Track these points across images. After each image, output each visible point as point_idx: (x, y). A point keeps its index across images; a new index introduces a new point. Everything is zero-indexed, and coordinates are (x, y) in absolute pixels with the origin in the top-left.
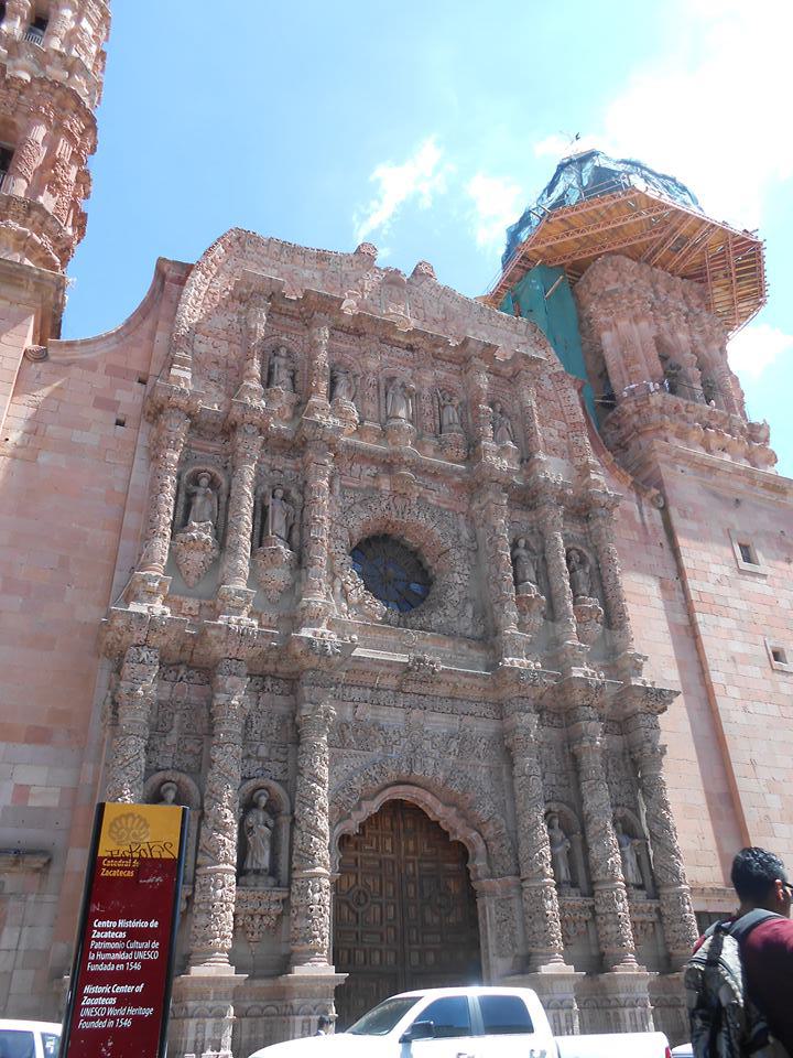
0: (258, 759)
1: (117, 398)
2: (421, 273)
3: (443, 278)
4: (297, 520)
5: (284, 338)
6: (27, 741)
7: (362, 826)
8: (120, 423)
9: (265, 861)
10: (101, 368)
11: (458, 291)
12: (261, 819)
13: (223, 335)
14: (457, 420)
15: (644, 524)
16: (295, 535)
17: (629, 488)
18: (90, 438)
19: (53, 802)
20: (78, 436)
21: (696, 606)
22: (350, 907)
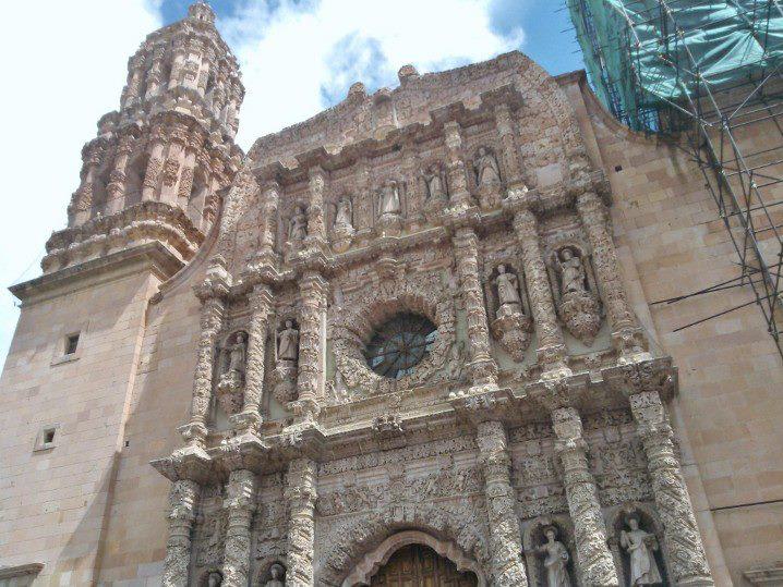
2: (407, 74)
5: (300, 199)
6: (154, 561)
15: (681, 175)
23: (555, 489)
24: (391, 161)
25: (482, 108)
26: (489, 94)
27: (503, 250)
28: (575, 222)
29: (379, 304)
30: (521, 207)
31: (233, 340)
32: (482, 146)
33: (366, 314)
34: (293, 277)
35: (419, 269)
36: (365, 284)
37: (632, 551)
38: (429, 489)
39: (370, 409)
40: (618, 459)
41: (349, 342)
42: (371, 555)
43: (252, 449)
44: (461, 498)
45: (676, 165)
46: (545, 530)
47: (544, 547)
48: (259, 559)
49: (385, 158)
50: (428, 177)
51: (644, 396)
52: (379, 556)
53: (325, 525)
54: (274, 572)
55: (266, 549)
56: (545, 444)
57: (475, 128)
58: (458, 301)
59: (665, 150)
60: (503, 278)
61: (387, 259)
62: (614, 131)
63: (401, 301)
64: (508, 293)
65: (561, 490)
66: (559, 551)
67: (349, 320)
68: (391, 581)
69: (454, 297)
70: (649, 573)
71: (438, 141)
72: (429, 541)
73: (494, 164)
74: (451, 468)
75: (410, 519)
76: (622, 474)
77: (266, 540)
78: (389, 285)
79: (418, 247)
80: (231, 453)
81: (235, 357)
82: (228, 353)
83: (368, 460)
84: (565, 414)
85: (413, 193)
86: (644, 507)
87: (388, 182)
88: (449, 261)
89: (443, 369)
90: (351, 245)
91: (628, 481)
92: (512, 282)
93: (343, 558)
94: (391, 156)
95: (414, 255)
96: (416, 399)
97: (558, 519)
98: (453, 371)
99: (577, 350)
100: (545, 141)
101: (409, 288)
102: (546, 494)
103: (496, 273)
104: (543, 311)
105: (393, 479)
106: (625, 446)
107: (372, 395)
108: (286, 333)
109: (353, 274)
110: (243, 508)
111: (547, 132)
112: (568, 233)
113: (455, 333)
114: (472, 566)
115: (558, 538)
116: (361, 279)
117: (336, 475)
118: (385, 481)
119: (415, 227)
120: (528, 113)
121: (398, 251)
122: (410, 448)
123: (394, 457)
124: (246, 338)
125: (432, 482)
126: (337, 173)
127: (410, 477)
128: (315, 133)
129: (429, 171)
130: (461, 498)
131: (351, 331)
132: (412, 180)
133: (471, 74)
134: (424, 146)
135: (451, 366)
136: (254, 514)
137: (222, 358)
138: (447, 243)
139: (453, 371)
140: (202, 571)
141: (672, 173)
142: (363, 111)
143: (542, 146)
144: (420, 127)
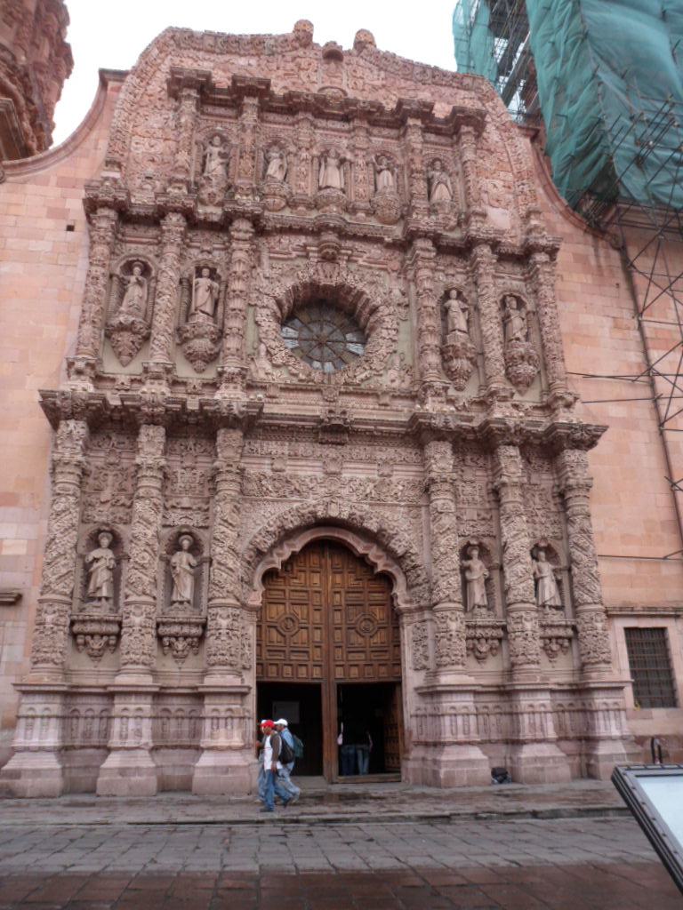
0: (183, 508)
1: (67, 206)
2: (364, 42)
3: (383, 45)
4: (222, 295)
5: (219, 128)
7: (284, 564)
8: (70, 228)
9: (187, 594)
10: (53, 180)
11: (398, 54)
12: (184, 560)
13: (159, 134)
14: (391, 183)
15: (599, 266)
16: (220, 309)
17: (585, 231)
18: (43, 246)
19: (22, 551)
20: (35, 246)
21: (650, 343)
22: (278, 631)
23: (483, 515)
24: (337, 130)
25: (447, 121)
26: (462, 110)
27: (453, 275)
28: (523, 274)
29: (313, 286)
30: (486, 242)
31: (128, 268)
32: (439, 160)
33: (295, 288)
34: (215, 219)
35: (361, 261)
36: (298, 256)
37: (542, 578)
38: (368, 491)
39: (301, 395)
40: (537, 499)
41: (274, 315)
42: (291, 542)
43: (179, 406)
44: (397, 505)
45: (597, 256)
46: (469, 549)
47: (470, 562)
48: (165, 526)
49: (330, 124)
50: (379, 168)
51: (577, 452)
52: (298, 544)
53: (248, 505)
54: (186, 543)
55: (177, 518)
56: (479, 473)
57: (432, 137)
58: (401, 310)
59: (590, 238)
60: (454, 304)
61: (331, 237)
62: (553, 202)
63: (341, 287)
64: (461, 322)
65: (488, 517)
66: (481, 568)
67: (280, 292)
68: (300, 571)
69: (399, 305)
70: (554, 598)
71: (394, 132)
72: (350, 539)
73: (449, 183)
74: (389, 476)
75: (345, 516)
76: (539, 513)
77: (173, 507)
78: (328, 267)
79: (365, 239)
80: (154, 405)
81: (135, 293)
82: (123, 285)
83: (302, 448)
84: (513, 451)
85: (361, 177)
86: (554, 544)
87: (332, 153)
88: (396, 265)
89: (381, 375)
90: (284, 207)
91: (543, 520)
92: (464, 310)
93: (270, 541)
94: (338, 125)
95: (358, 245)
96: (353, 398)
97: (486, 541)
98: (393, 381)
99: (517, 397)
100: (499, 183)
102: (475, 518)
103: (447, 296)
104: (495, 351)
105: (329, 474)
106: (543, 489)
107: (301, 380)
108: (204, 282)
109: (285, 240)
110: (161, 468)
111: (502, 173)
112: (515, 283)
113: (394, 341)
114: (393, 570)
115: (480, 557)
116: (294, 250)
117: (262, 457)
118: (320, 475)
119: (361, 215)
120: (485, 147)
121: (342, 234)
122: (349, 447)
123: (332, 452)
124: (146, 270)
125: (372, 485)
126: (272, 117)
127: (346, 475)
128: (245, 55)
129: (377, 158)
130: (397, 505)
131: (279, 303)
132: (361, 162)
133: (434, 77)
134: (375, 131)
135: (393, 374)
136: (166, 477)
137: (115, 287)
138: (404, 245)
139: (393, 381)
140: (91, 528)
141: (593, 262)
142: (308, 58)
143: (495, 186)
144: (380, 108)
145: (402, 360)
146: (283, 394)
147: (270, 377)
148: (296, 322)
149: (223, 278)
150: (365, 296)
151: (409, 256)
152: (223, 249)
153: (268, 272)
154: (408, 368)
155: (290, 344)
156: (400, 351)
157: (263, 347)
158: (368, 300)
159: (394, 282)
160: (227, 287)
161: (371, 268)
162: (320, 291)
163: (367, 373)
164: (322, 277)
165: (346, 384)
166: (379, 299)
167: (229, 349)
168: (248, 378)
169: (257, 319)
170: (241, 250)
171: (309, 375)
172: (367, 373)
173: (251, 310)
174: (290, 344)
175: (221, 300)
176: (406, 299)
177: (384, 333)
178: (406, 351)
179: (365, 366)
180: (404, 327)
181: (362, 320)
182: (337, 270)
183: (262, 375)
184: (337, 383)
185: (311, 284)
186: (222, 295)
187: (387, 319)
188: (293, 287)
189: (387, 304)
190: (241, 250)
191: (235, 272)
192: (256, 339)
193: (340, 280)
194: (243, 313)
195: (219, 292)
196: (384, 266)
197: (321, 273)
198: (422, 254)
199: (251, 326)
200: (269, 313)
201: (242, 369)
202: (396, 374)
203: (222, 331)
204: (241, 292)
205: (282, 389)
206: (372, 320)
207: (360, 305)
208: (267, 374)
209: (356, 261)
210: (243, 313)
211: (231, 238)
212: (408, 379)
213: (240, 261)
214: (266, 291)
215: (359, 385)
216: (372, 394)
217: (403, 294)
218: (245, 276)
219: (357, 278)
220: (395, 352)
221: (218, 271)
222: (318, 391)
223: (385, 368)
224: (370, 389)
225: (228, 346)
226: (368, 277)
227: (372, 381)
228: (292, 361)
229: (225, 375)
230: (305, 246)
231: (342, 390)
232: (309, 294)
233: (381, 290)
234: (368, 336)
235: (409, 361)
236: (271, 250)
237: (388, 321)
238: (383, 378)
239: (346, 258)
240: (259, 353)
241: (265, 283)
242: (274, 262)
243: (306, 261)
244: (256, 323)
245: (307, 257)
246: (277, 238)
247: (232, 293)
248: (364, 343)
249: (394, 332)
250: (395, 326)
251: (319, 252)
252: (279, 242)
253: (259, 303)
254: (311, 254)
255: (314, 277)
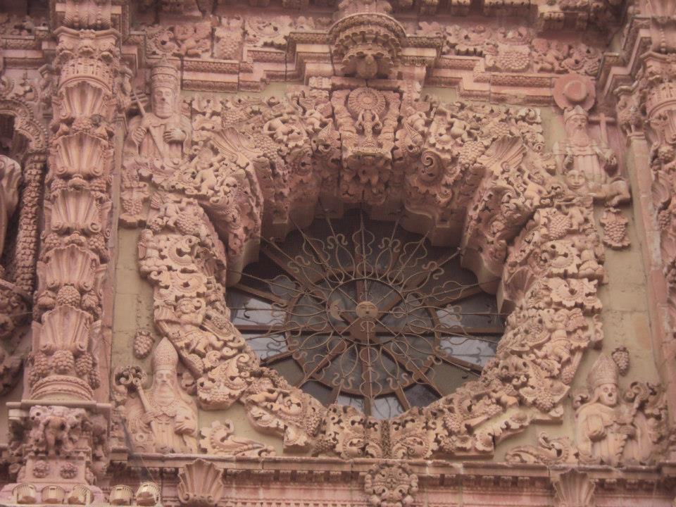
33: (267, 171)
35: (468, 81)
36: (272, 76)
41: (201, 251)
58: (608, 217)
69: (599, 203)
78: (365, 101)
88: (581, 85)
89: (557, 422)
98: (597, 439)
101: (437, 127)
107: (294, 449)
113: (591, 313)
116: (259, 59)
131: (215, 216)
135: (593, 416)
139: (597, 439)
145: (622, 372)
146: (233, 493)
147: (191, 442)
148: (281, 286)
149: (33, 145)
150: (487, 183)
151: (618, 52)
152: (34, 64)
153: (178, 125)
154: (643, 394)
155: (261, 348)
156: (611, 345)
157: (165, 353)
158: (499, 192)
159: (578, 137)
160: (45, 169)
161: (501, 100)
162: (347, 178)
163: (510, 417)
164: (347, 129)
165: (442, 453)
166: (532, 189)
167: (49, 353)
168: (114, 444)
169: (146, 265)
170: (88, 54)
171: (320, 430)
172: (511, 416)
173: (129, 238)
174: (261, 348)
175: (28, 210)
176: (622, 185)
177: (559, 290)
178: (632, 342)
179: (505, 398)
180: (618, 267)
181: (486, 261)
182: (394, 110)
183: (163, 437)
184: (410, 454)
185: (316, 154)
186: (30, 195)
187: (561, 247)
188: (258, 165)
189: (558, 200)
190: (88, 54)
191: (69, 122)
192: (144, 322)
193: (406, 139)
194: (98, 242)
195: (22, 186)
196: (545, 92)
197: (344, 118)
198: (657, 37)
199: (128, 285)
200: (186, 248)
201: (89, 409)
202: (607, 415)
203: (27, 302)
204: (89, 177)
205: (228, 477)
206: (515, 255)
207: (473, 214)
208: (180, 433)
209: (453, 83)
210: (98, 242)
211: (59, 20)
212: (646, 427)
213: (83, 86)
214: (173, 180)
215: (485, 455)
216: (533, 481)
217: (611, 170)
218: (101, 130)
219: (455, 130)
220: (598, 346)
221: (19, 124)
222: (351, 478)
223: (568, 400)
224: (524, 467)
225: (46, 340)
226: (492, 126)
227: (526, 442)
228: (262, 389)
229: (35, 433)
230: (290, 44)
231: (429, 472)
232: (313, 191)
233: (539, 162)
234: (509, 307)
235: (645, 373)
236: (185, 60)
237: (570, 256)
238: (566, 431)
239: (420, 71)
240: (152, 372)
241: (170, 157)
242: (197, 95)
243: (294, 89)
244: (144, 277)
245: (300, 77)
246: (207, 25)
247: (59, 183)
248: (493, 332)
249: (590, 287)
250: (591, 266)
251: (332, 58)
252: (212, 36)
253: (152, 218)
254: (310, 67)
255: (323, 134)
